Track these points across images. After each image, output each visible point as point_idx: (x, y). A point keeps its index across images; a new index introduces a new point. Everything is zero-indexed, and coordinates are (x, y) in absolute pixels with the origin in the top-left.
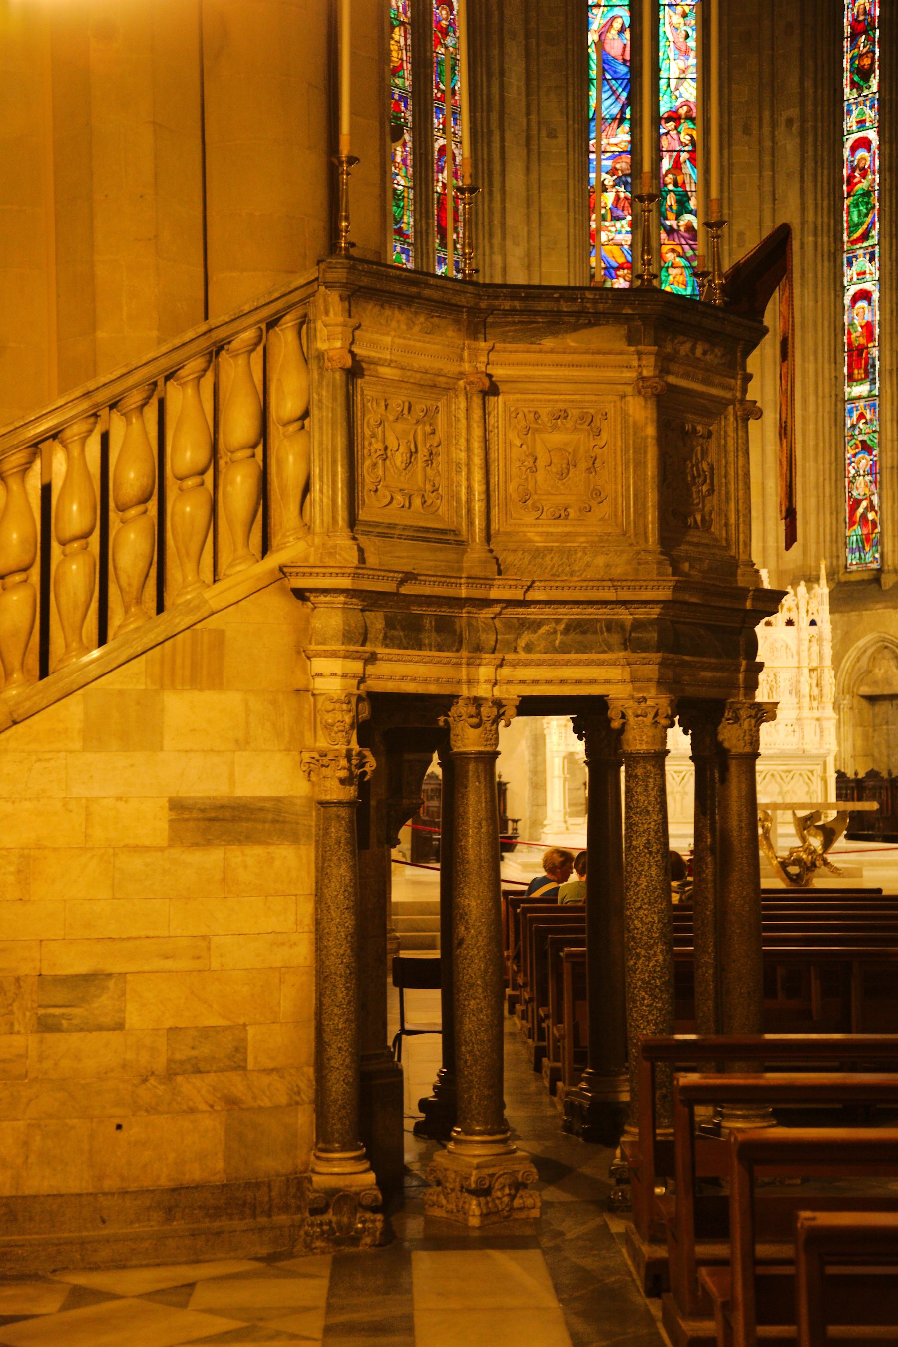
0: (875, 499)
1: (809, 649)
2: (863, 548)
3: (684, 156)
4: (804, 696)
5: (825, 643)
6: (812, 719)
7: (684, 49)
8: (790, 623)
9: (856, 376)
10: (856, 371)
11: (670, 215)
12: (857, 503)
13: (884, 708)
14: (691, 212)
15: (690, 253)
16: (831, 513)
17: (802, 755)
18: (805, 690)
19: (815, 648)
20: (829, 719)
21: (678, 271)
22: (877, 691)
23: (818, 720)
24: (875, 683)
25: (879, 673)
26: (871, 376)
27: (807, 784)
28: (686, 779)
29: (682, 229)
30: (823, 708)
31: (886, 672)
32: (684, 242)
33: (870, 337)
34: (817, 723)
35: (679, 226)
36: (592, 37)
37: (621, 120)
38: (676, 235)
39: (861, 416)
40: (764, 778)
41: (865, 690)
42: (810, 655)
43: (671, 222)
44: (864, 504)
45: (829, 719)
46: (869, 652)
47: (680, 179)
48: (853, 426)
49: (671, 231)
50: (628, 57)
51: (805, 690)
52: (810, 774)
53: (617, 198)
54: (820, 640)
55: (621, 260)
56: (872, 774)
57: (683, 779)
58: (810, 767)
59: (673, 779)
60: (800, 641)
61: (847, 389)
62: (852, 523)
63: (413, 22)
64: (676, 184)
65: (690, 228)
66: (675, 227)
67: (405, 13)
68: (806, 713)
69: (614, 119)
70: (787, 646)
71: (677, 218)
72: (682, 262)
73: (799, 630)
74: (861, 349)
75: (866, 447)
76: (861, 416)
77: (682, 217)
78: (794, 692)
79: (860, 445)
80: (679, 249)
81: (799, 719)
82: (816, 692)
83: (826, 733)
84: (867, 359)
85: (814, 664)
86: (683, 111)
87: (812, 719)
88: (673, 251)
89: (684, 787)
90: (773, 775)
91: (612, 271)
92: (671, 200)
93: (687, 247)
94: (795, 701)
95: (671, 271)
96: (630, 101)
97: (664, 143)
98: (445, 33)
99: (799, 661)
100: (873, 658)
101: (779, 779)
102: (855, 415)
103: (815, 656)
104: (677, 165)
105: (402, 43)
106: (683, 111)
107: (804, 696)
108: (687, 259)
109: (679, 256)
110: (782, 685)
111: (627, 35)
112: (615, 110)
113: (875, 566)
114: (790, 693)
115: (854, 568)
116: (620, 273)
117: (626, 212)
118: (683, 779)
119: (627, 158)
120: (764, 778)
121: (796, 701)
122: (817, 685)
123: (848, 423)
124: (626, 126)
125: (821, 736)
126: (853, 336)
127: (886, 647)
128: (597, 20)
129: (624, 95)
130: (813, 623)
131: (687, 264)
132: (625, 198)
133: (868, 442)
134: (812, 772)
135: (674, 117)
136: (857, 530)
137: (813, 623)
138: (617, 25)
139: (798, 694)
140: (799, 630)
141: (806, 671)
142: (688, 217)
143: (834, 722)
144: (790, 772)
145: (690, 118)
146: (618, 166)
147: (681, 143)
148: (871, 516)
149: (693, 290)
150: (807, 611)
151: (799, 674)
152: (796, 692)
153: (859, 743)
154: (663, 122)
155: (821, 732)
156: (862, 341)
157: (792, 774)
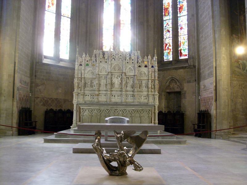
0: (171, 45)
1: (151, 75)
2: (168, 55)
4: (149, 88)
5: (156, 73)
6: (151, 95)
9: (166, 15)
10: (166, 14)
12: (167, 45)
13: (172, 96)
16: (160, 47)
17: (147, 105)
18: (150, 86)
19: (153, 74)
20: (156, 95)
22: (171, 91)
23: (153, 95)
24: (170, 89)
25: (171, 86)
26: (170, 15)
27: (148, 114)
28: (110, 112)
30: (155, 92)
31: (173, 86)
33: (169, 6)
34: (153, 96)
39: (167, 24)
40: (135, 112)
41: (168, 91)
42: (151, 76)
44: (168, 45)
45: (156, 95)
46: (169, 81)
48: (166, 26)
51: (150, 86)
52: (149, 111)
54: (155, 71)
56: (169, 112)
57: (109, 112)
58: (149, 109)
59: (106, 111)
60: (149, 72)
61: (164, 18)
62: (165, 50)
68: (150, 93)
70: (145, 73)
73: (148, 68)
74: (167, 9)
75: (169, 31)
76: (167, 24)
78: (146, 87)
79: (167, 31)
81: (148, 95)
82: (153, 87)
83: (156, 99)
84: (169, 11)
87: (151, 95)
89: (109, 114)
90: (138, 111)
94: (147, 89)
99: (148, 78)
100: (170, 82)
101: (139, 112)
102: (166, 24)
103: (153, 76)
107: (149, 88)
110: (143, 84)
113: (171, 59)
114: (146, 87)
115: (166, 61)
118: (109, 112)
120: (135, 112)
121: (147, 89)
122: (153, 85)
123: (164, 26)
125: (154, 100)
126: (166, 6)
127: (173, 79)
130: (152, 67)
133: (169, 30)
134: (150, 110)
136: (167, 51)
137: (152, 67)
139: (148, 87)
140: (148, 68)
141: (150, 81)
143: (158, 96)
144: (143, 110)
148: (170, 48)
150: (151, 63)
151: (149, 82)
152: (147, 87)
153: (166, 104)
155: (154, 99)
156: (167, 7)
157: (143, 111)
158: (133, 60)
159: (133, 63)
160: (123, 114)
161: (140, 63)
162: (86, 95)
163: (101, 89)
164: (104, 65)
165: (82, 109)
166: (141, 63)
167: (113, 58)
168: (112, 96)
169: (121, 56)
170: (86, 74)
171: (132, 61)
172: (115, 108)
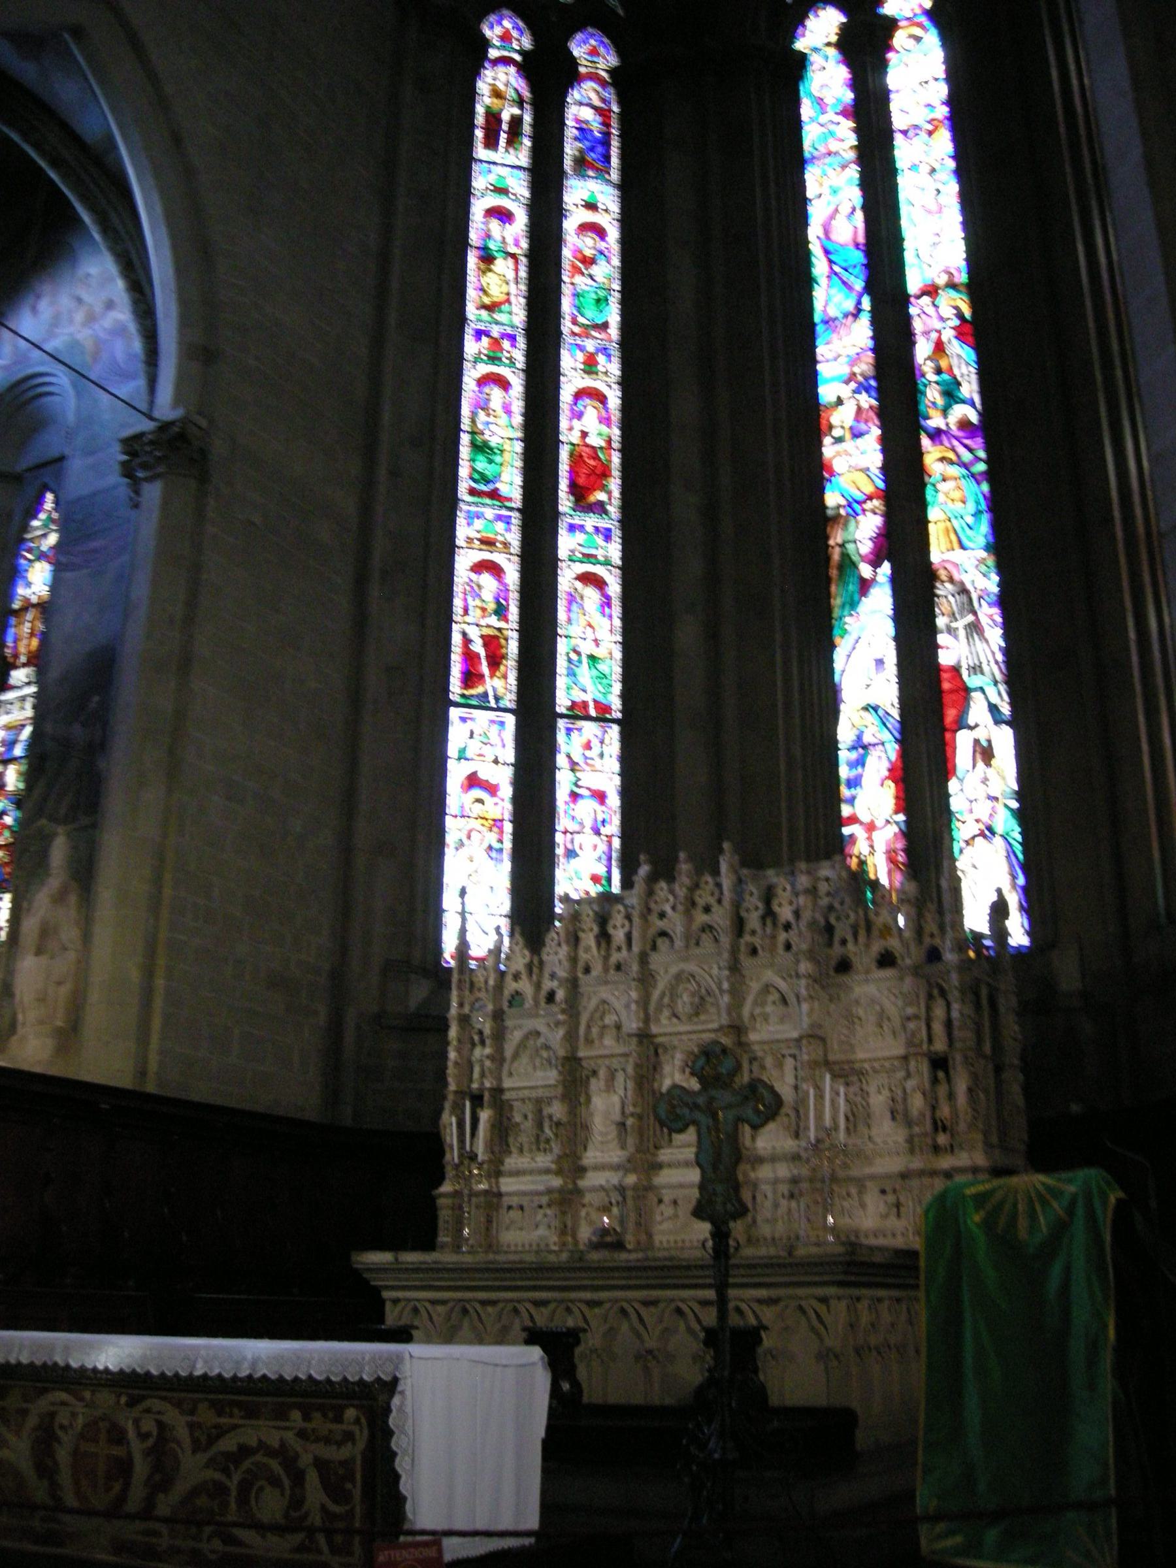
3: (948, 335)
7: (934, 208)
8: (886, 960)
11: (932, 412)
14: (963, 402)
15: (967, 456)
21: (950, 484)
29: (953, 427)
32: (955, 443)
35: (947, 424)
36: (814, 232)
37: (857, 313)
38: (944, 438)
43: (936, 421)
47: (943, 364)
49: (937, 435)
50: (861, 239)
53: (859, 409)
55: (869, 489)
63: (532, 255)
64: (939, 371)
65: (964, 424)
66: (944, 427)
67: (517, 244)
69: (846, 316)
71: (945, 412)
72: (955, 471)
77: (951, 411)
80: (951, 455)
85: (940, 1046)
86: (942, 280)
88: (942, 459)
91: (856, 506)
92: (933, 394)
93: (961, 450)
95: (942, 486)
96: (869, 288)
97: (918, 325)
98: (589, 262)
104: (939, 347)
105: (511, 275)
106: (942, 280)
108: (965, 466)
109: (951, 462)
111: (859, 216)
112: (850, 305)
116: (868, 505)
117: (870, 424)
119: (869, 357)
124: (865, 319)
128: (817, 214)
129: (859, 285)
131: (964, 471)
132: (871, 407)
135: (931, 291)
138: (845, 209)
142: (960, 411)
145: (952, 285)
146: (856, 370)
147: (942, 319)
149: (978, 503)
154: (912, 300)
158: (787, 927)
159: (788, 947)
160: (639, 1336)
161: (844, 942)
162: (510, 1208)
163: (591, 1156)
164: (604, 993)
165: (396, 1301)
166: (850, 946)
167: (663, 934)
168: (660, 1201)
169: (707, 909)
170: (506, 1066)
171: (782, 936)
172: (588, 1295)
